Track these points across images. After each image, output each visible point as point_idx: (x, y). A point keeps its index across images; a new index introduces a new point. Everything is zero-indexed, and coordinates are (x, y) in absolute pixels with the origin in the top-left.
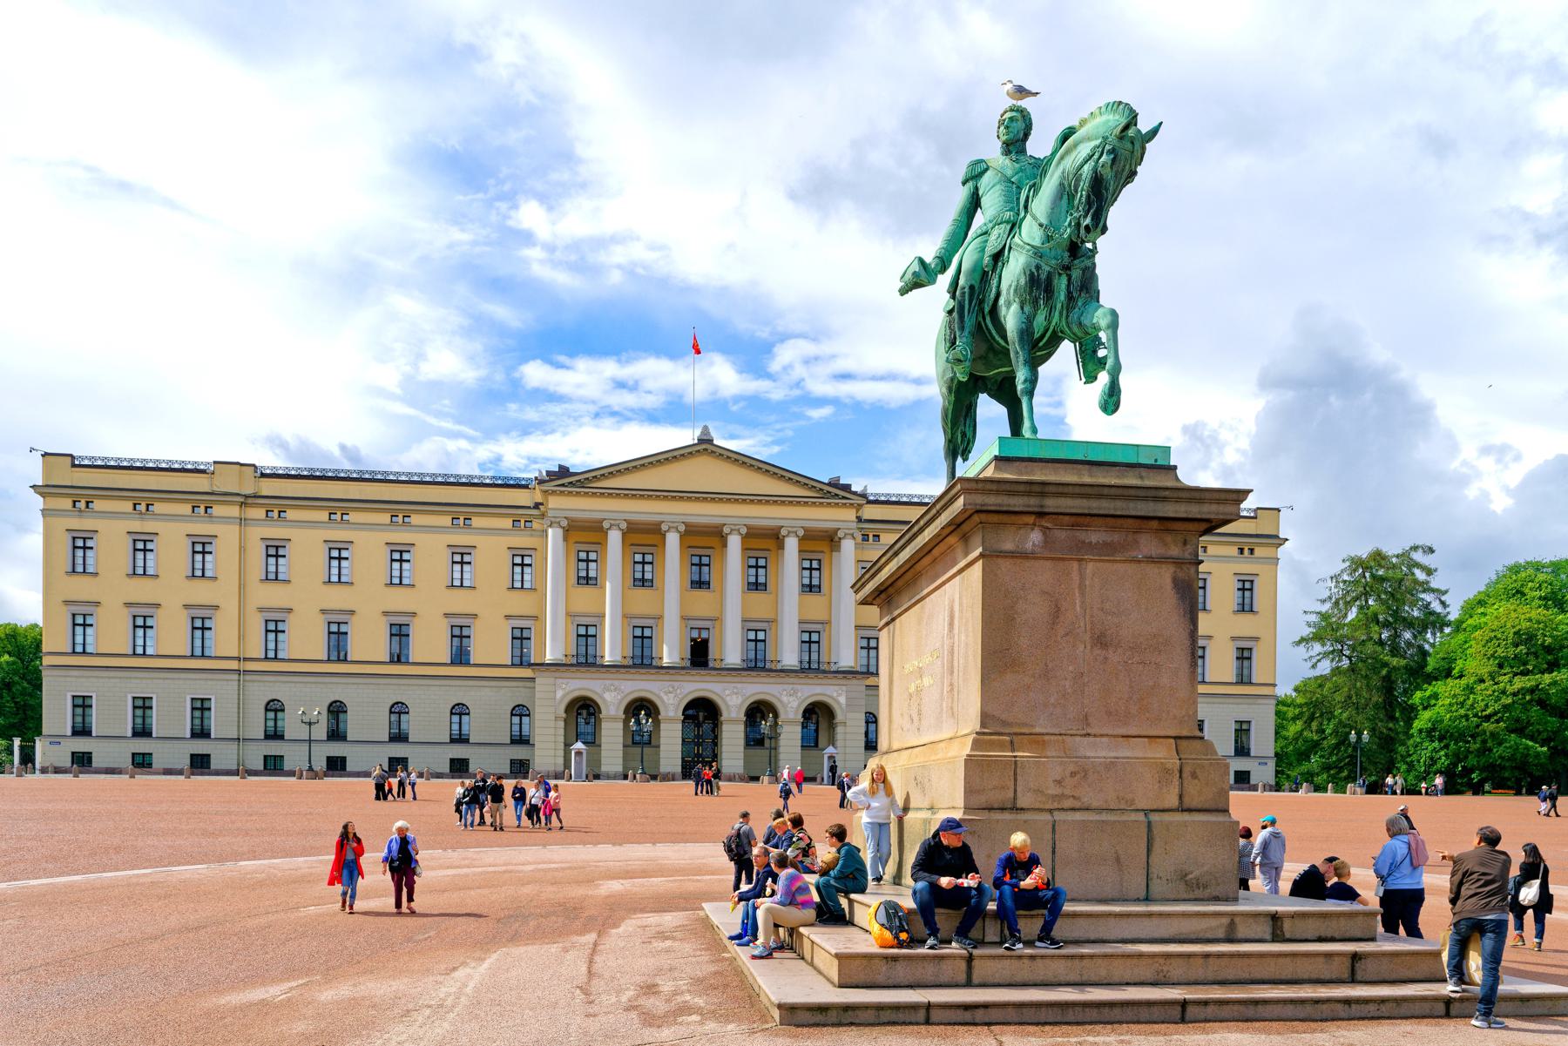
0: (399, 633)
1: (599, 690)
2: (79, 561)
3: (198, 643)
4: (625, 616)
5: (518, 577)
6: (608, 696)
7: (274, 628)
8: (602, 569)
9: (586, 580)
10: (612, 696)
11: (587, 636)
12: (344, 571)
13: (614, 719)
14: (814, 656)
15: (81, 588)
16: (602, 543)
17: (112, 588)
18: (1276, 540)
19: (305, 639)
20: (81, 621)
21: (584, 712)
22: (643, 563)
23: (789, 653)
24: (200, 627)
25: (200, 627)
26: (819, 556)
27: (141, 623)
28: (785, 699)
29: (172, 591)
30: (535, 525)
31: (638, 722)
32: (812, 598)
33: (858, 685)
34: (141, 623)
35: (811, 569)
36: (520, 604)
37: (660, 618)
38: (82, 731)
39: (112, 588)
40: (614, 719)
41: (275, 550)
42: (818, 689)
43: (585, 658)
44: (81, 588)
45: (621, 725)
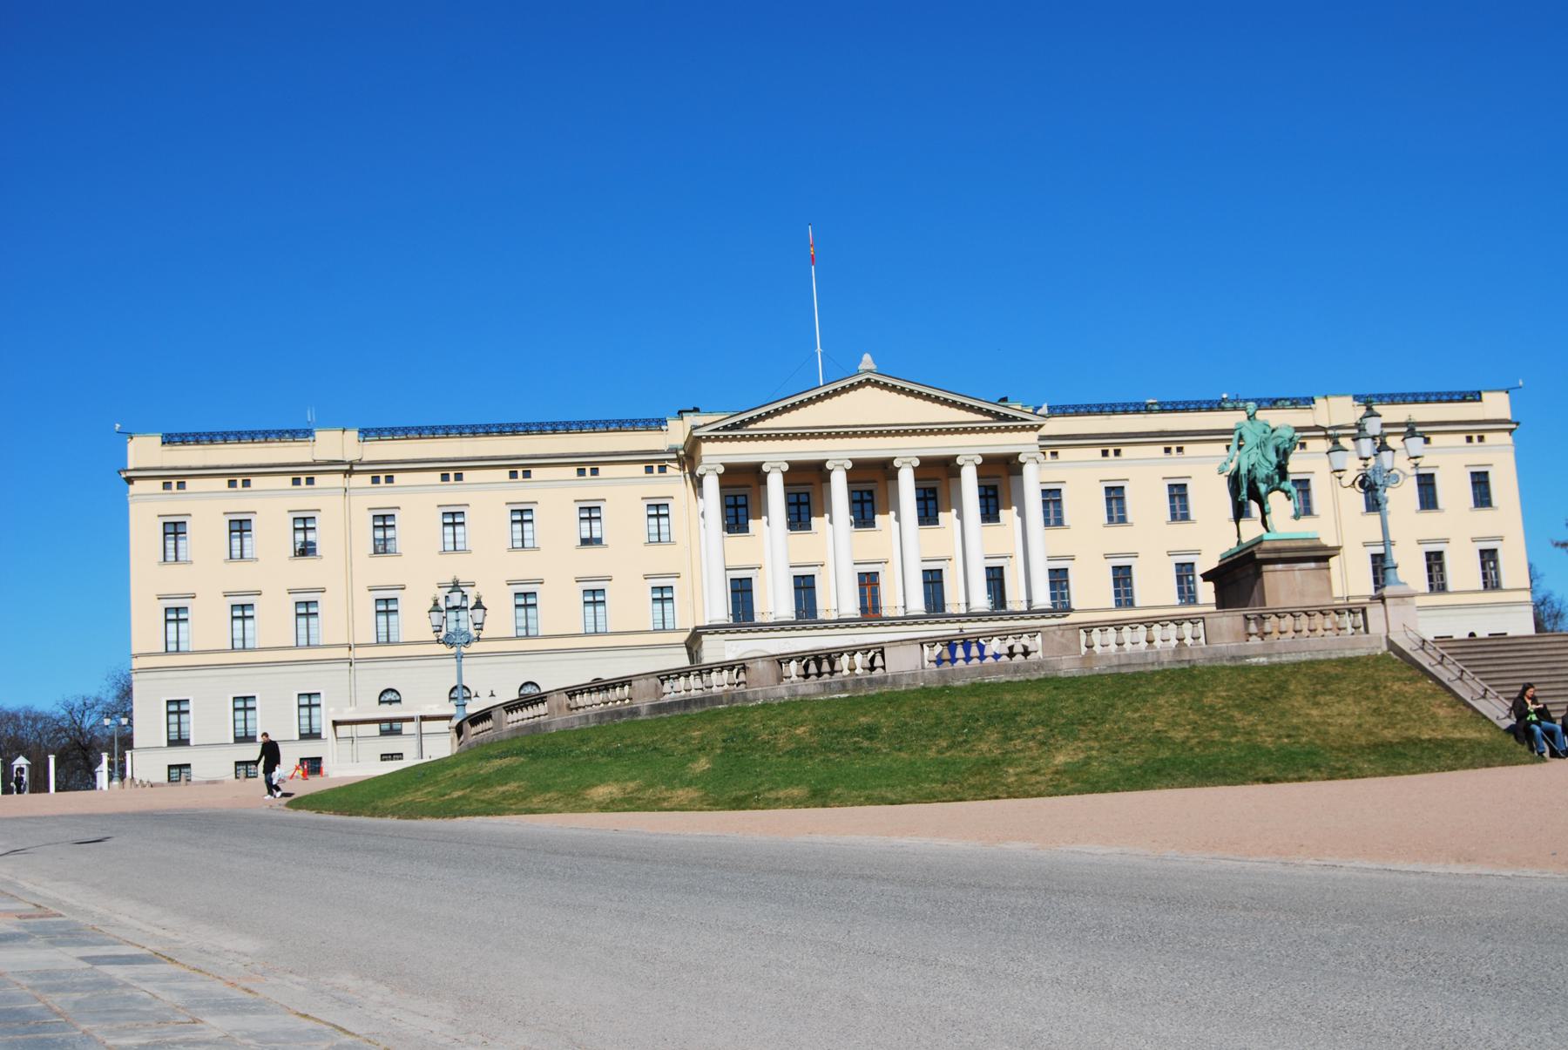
3: (302, 632)
25: (306, 610)
34: (242, 612)
38: (179, 741)
41: (383, 521)
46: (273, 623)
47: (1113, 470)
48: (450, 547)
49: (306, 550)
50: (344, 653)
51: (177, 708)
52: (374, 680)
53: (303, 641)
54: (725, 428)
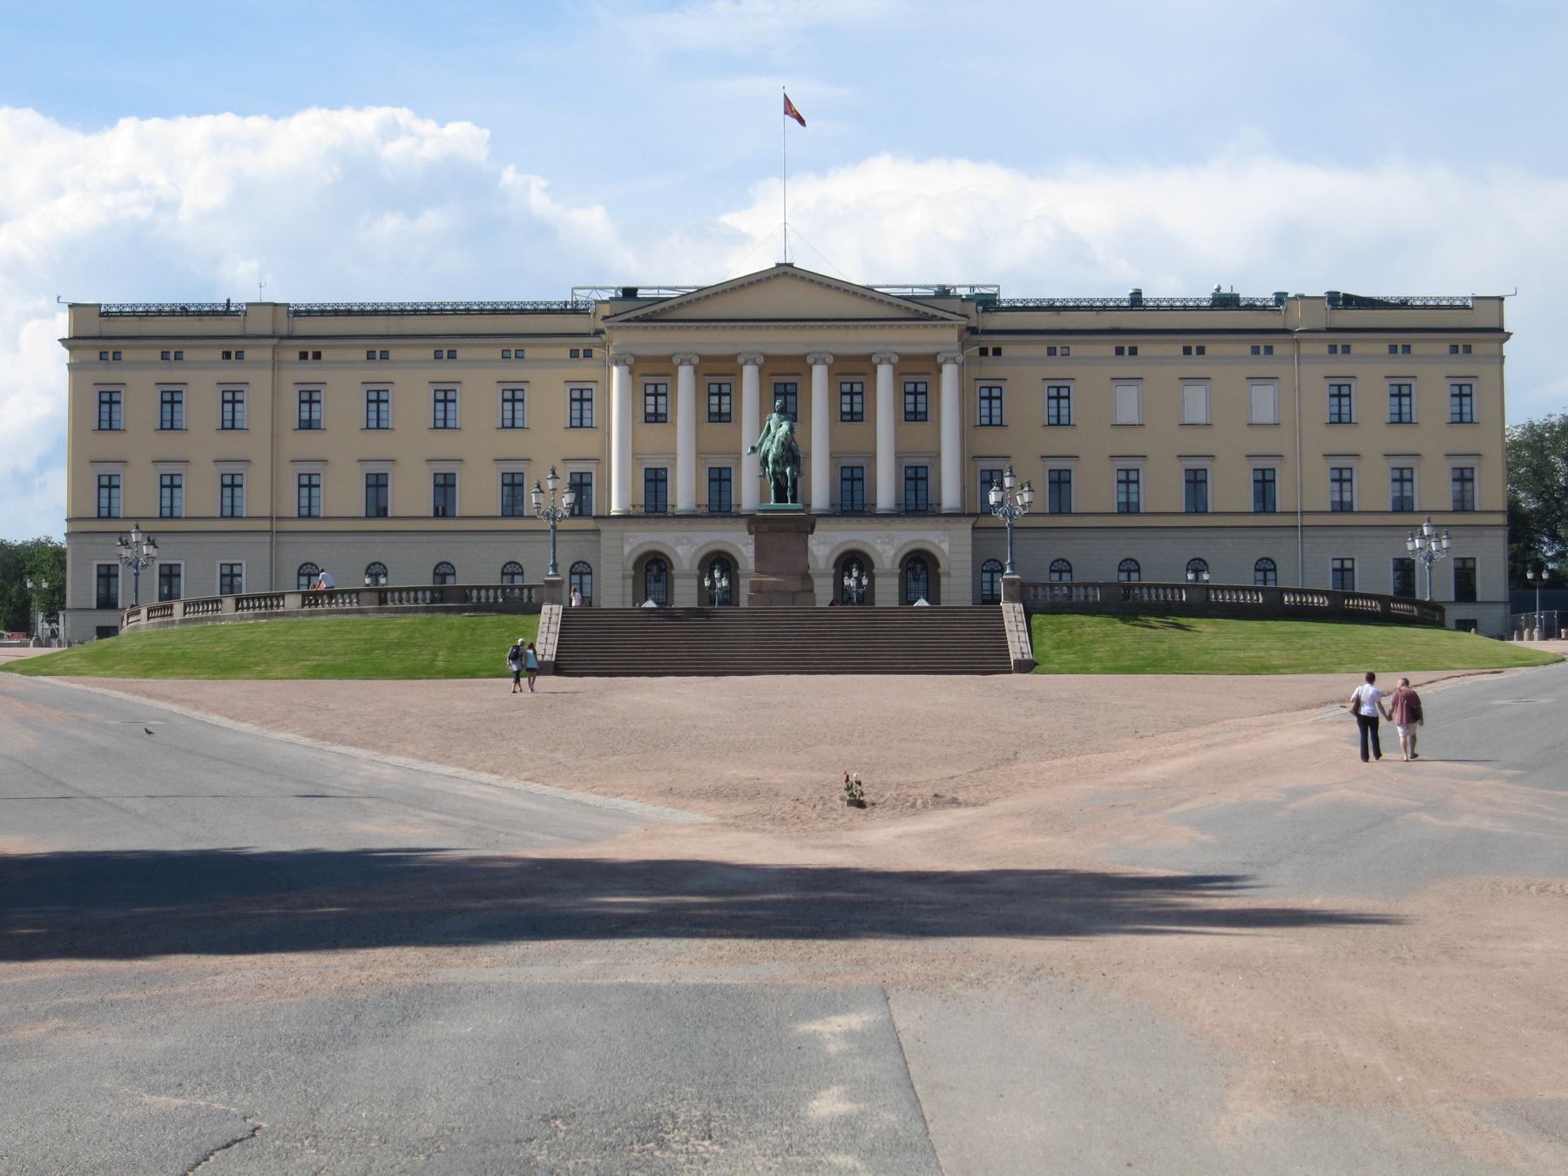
0: (445, 486)
2: (105, 416)
3: (227, 502)
4: (698, 453)
5: (576, 414)
6: (681, 550)
9: (656, 418)
10: (685, 548)
11: (656, 481)
12: (383, 415)
13: (687, 576)
14: (921, 495)
16: (673, 375)
18: (1498, 333)
19: (343, 495)
20: (108, 485)
21: (655, 569)
22: (720, 394)
23: (885, 494)
25: (231, 485)
27: (171, 484)
28: (879, 548)
29: (202, 444)
30: (597, 352)
31: (712, 577)
33: (964, 529)
34: (171, 484)
36: (580, 443)
40: (687, 576)
41: (309, 399)
44: (109, 445)
45: (695, 582)
46: (201, 496)
47: (1058, 369)
48: (373, 424)
50: (266, 525)
51: (107, 575)
52: (295, 554)
53: (227, 512)
54: (637, 319)
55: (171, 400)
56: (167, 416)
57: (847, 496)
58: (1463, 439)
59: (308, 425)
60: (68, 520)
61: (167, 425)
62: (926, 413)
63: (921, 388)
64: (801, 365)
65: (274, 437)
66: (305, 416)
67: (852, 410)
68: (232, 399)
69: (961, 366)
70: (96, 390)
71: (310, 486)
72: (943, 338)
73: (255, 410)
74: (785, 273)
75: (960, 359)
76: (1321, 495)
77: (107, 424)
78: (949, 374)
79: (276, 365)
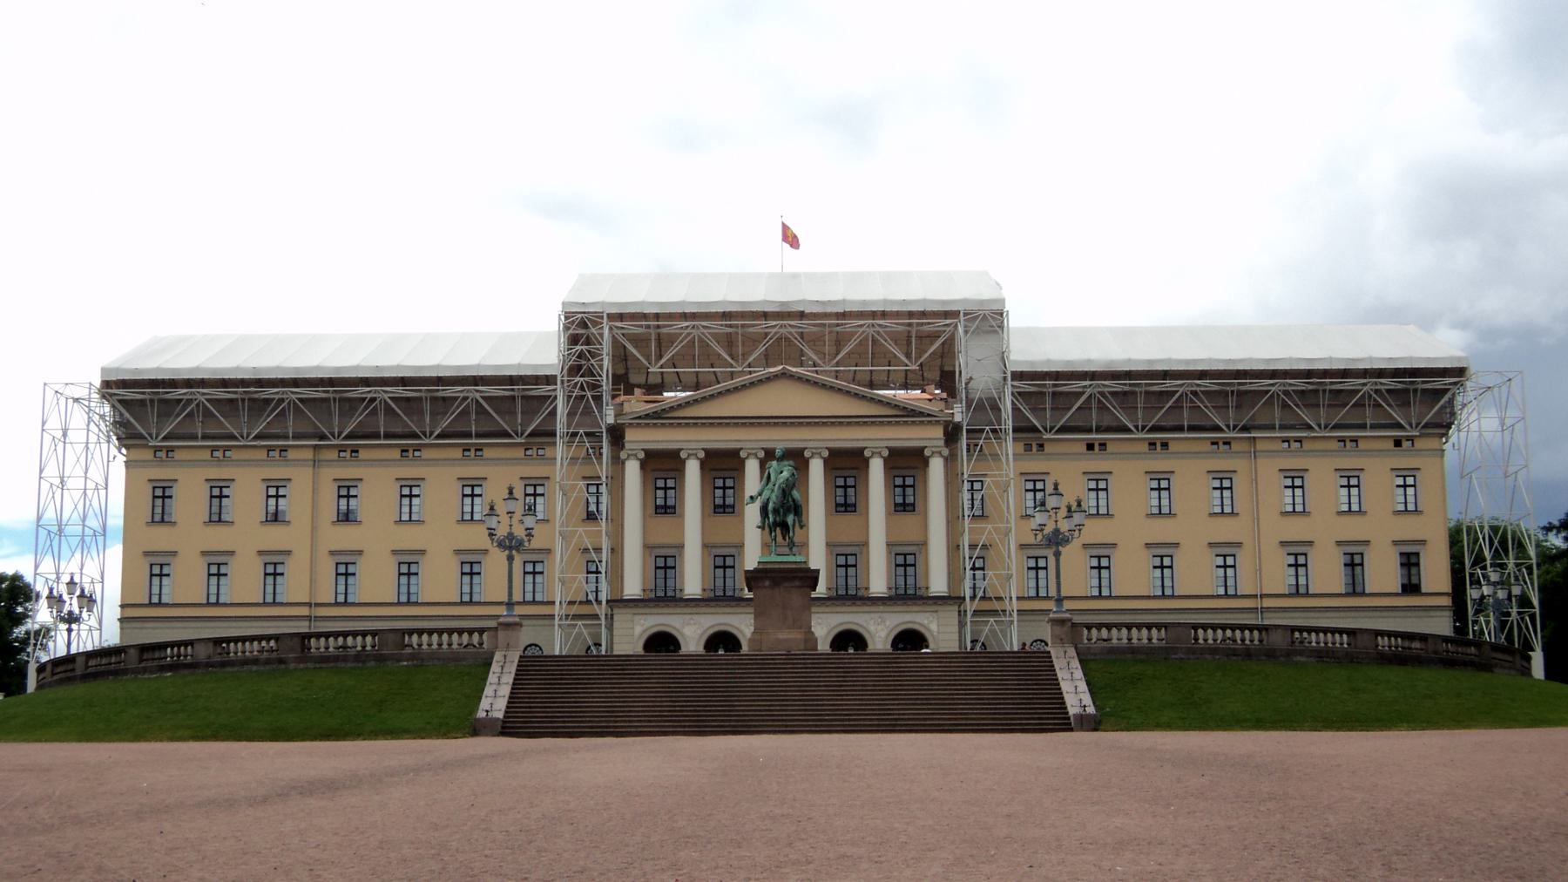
1: (677, 625)
2: (158, 510)
3: (270, 589)
4: (706, 546)
7: (345, 572)
8: (680, 496)
10: (692, 633)
12: (414, 509)
14: (910, 581)
15: (161, 538)
17: (190, 533)
23: (878, 582)
24: (273, 573)
25: (273, 573)
26: (912, 472)
27: (217, 572)
28: (872, 628)
29: (246, 535)
32: (907, 519)
34: (217, 572)
35: (904, 486)
37: (742, 546)
39: (190, 533)
41: (346, 490)
42: (908, 617)
43: (664, 595)
44: (161, 538)
46: (244, 584)
48: (405, 517)
49: (275, 518)
50: (304, 611)
53: (269, 599)
54: (647, 416)
55: (218, 493)
56: (215, 509)
57: (842, 581)
58: (1409, 529)
59: (346, 517)
60: (122, 606)
61: (215, 518)
62: (913, 505)
63: (909, 481)
64: (798, 458)
65: (314, 529)
66: (343, 507)
67: (846, 503)
68: (275, 489)
69: (951, 461)
70: (150, 486)
71: (347, 574)
72: (932, 436)
73: (296, 503)
74: (784, 375)
75: (946, 452)
76: (1278, 578)
77: (161, 519)
78: (936, 467)
79: (315, 463)
